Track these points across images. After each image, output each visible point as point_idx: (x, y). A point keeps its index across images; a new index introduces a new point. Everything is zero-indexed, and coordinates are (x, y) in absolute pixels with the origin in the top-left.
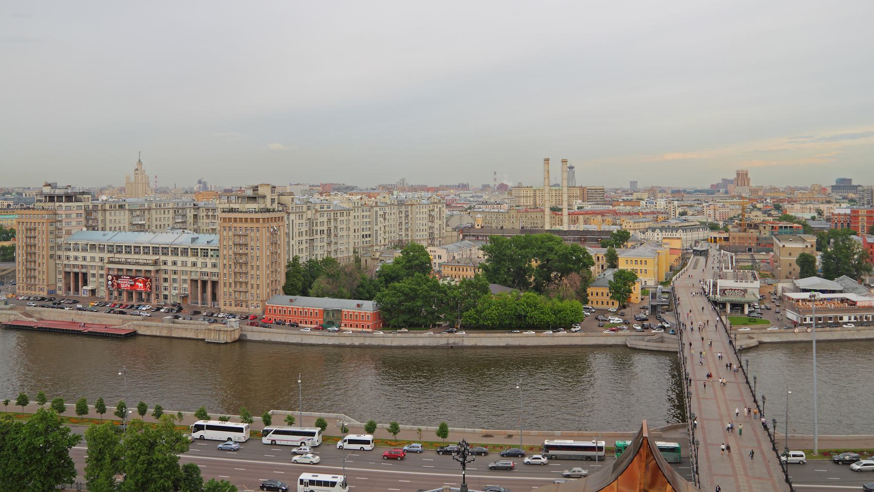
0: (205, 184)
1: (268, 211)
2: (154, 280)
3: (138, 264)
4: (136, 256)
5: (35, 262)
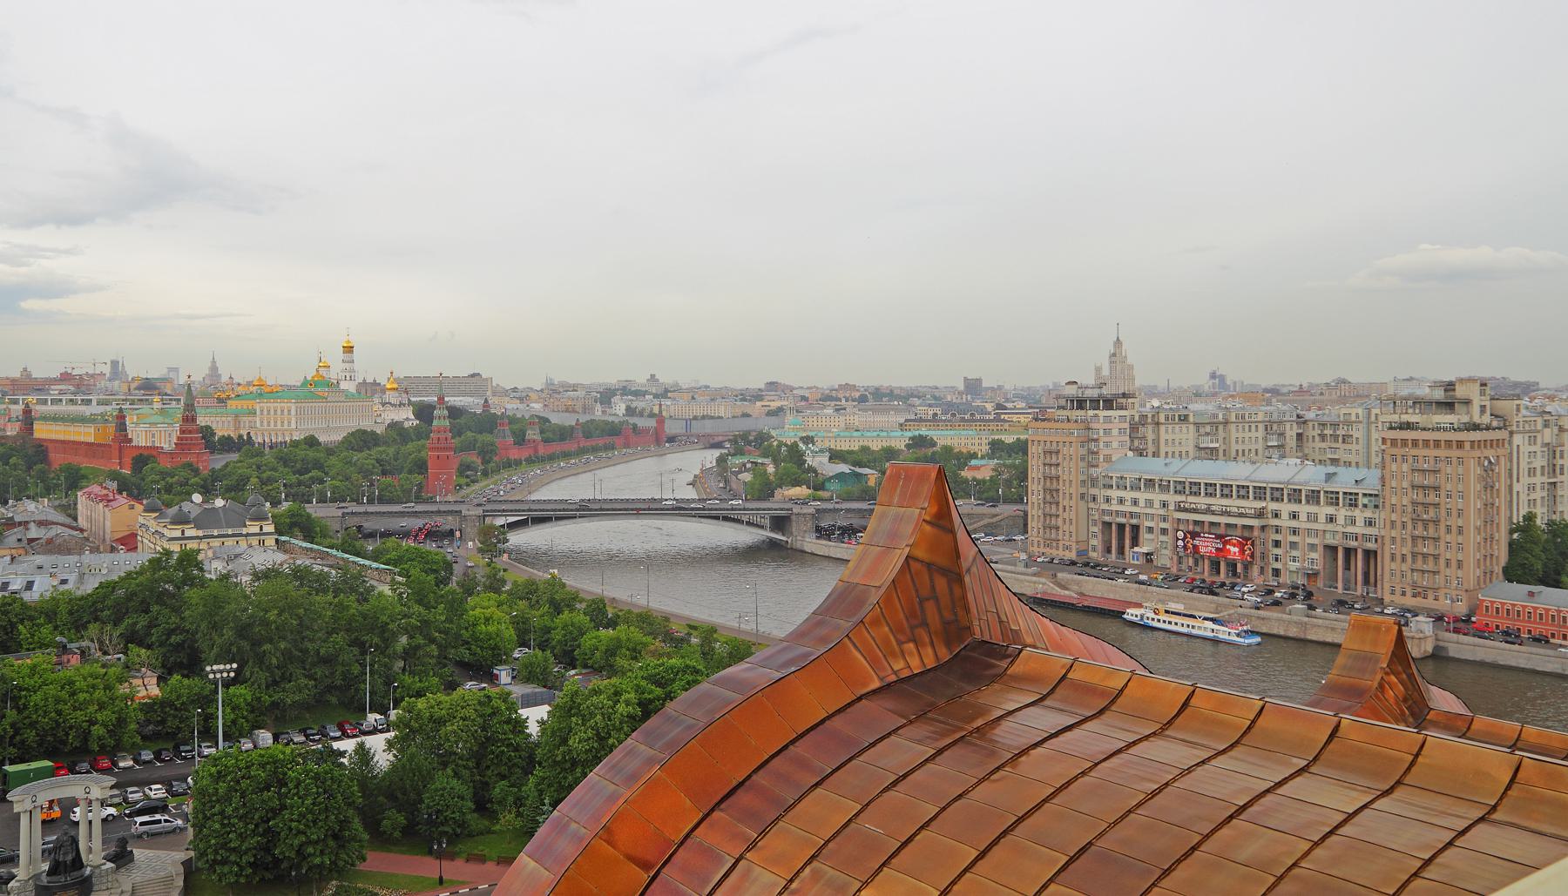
0: (1222, 378)
1: (1476, 427)
2: (1257, 542)
3: (1229, 514)
4: (1225, 502)
5: (1057, 504)
